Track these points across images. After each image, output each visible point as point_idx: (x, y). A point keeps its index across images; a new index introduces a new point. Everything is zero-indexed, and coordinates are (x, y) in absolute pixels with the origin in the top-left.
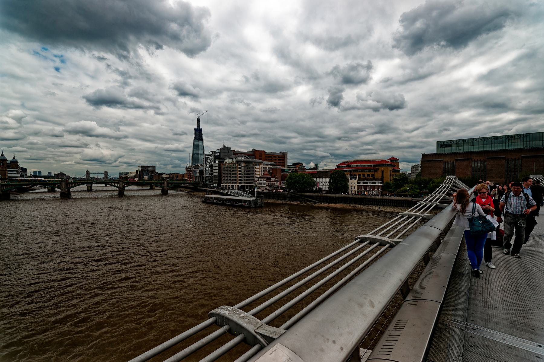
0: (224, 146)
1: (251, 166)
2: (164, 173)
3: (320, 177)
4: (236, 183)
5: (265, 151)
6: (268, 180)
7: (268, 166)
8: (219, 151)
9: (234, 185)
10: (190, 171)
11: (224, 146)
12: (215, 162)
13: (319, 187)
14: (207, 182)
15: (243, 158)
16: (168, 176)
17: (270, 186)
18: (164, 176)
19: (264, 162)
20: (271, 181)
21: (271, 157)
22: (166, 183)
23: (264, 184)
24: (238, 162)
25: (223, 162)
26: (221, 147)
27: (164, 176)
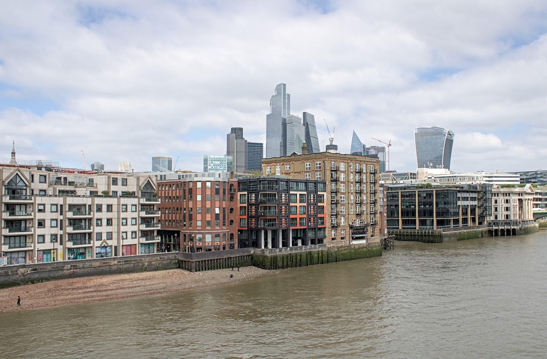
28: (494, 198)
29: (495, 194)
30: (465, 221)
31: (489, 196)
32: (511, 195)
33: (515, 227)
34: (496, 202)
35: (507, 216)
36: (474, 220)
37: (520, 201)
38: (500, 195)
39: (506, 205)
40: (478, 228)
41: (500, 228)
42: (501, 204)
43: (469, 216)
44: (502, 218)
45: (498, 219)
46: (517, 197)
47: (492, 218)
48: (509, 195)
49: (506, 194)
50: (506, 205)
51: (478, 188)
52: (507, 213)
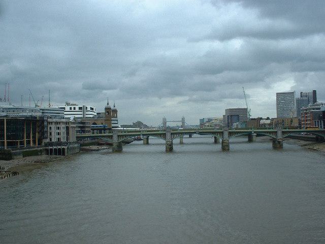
2: (261, 119)
10: (306, 113)
16: (268, 122)
18: (262, 122)
27: (262, 122)
28: (49, 126)
29: (50, 123)
30: (28, 142)
31: (45, 124)
32: (61, 124)
34: (50, 128)
35: (59, 138)
36: (34, 142)
37: (67, 128)
38: (53, 124)
39: (58, 131)
40: (38, 147)
42: (54, 130)
43: (31, 139)
46: (64, 126)
47: (48, 140)
50: (58, 131)
51: (38, 118)
52: (58, 136)
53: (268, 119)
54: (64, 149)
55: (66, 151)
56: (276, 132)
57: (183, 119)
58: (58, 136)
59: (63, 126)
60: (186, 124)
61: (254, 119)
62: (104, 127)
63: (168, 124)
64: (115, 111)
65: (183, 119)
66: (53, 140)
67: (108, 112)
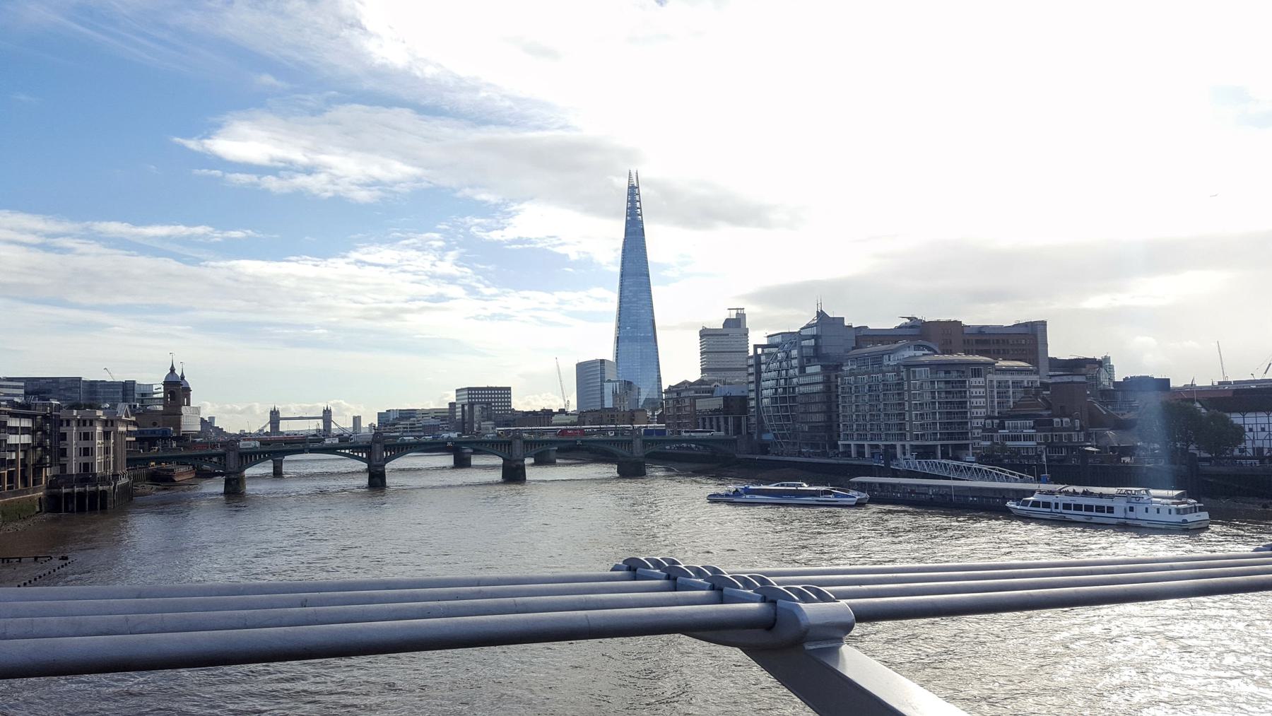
0: (821, 315)
1: (954, 376)
2: (547, 414)
3: (1256, 409)
4: (902, 437)
5: (965, 322)
6: (1041, 424)
7: (1009, 378)
8: (814, 331)
9: (898, 444)
11: (821, 315)
12: (802, 369)
13: (1258, 444)
14: (768, 437)
15: (919, 353)
17: (1051, 447)
19: (1002, 363)
20: (1052, 430)
21: (986, 342)
22: (638, 443)
23: (1030, 438)
24: (909, 366)
25: (838, 367)
26: (809, 316)
27: (555, 419)
33: (106, 488)
35: (86, 465)
37: (106, 435)
38: (74, 423)
41: (76, 489)
42: (74, 444)
44: (74, 469)
45: (68, 472)
48: (91, 424)
49: (85, 422)
52: (84, 460)
53: (562, 411)
54: (104, 492)
55: (109, 499)
56: (630, 442)
57: (327, 414)
58: (84, 460)
59: (99, 429)
60: (333, 426)
61: (534, 413)
62: (165, 432)
63: (284, 427)
64: (188, 390)
65: (327, 414)
66: (74, 469)
67: (172, 393)
